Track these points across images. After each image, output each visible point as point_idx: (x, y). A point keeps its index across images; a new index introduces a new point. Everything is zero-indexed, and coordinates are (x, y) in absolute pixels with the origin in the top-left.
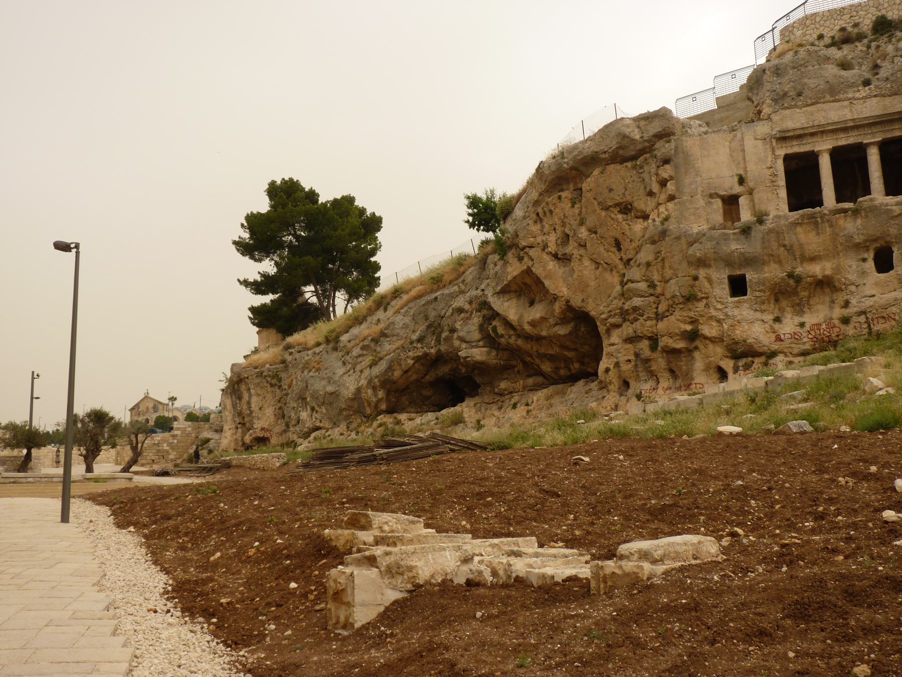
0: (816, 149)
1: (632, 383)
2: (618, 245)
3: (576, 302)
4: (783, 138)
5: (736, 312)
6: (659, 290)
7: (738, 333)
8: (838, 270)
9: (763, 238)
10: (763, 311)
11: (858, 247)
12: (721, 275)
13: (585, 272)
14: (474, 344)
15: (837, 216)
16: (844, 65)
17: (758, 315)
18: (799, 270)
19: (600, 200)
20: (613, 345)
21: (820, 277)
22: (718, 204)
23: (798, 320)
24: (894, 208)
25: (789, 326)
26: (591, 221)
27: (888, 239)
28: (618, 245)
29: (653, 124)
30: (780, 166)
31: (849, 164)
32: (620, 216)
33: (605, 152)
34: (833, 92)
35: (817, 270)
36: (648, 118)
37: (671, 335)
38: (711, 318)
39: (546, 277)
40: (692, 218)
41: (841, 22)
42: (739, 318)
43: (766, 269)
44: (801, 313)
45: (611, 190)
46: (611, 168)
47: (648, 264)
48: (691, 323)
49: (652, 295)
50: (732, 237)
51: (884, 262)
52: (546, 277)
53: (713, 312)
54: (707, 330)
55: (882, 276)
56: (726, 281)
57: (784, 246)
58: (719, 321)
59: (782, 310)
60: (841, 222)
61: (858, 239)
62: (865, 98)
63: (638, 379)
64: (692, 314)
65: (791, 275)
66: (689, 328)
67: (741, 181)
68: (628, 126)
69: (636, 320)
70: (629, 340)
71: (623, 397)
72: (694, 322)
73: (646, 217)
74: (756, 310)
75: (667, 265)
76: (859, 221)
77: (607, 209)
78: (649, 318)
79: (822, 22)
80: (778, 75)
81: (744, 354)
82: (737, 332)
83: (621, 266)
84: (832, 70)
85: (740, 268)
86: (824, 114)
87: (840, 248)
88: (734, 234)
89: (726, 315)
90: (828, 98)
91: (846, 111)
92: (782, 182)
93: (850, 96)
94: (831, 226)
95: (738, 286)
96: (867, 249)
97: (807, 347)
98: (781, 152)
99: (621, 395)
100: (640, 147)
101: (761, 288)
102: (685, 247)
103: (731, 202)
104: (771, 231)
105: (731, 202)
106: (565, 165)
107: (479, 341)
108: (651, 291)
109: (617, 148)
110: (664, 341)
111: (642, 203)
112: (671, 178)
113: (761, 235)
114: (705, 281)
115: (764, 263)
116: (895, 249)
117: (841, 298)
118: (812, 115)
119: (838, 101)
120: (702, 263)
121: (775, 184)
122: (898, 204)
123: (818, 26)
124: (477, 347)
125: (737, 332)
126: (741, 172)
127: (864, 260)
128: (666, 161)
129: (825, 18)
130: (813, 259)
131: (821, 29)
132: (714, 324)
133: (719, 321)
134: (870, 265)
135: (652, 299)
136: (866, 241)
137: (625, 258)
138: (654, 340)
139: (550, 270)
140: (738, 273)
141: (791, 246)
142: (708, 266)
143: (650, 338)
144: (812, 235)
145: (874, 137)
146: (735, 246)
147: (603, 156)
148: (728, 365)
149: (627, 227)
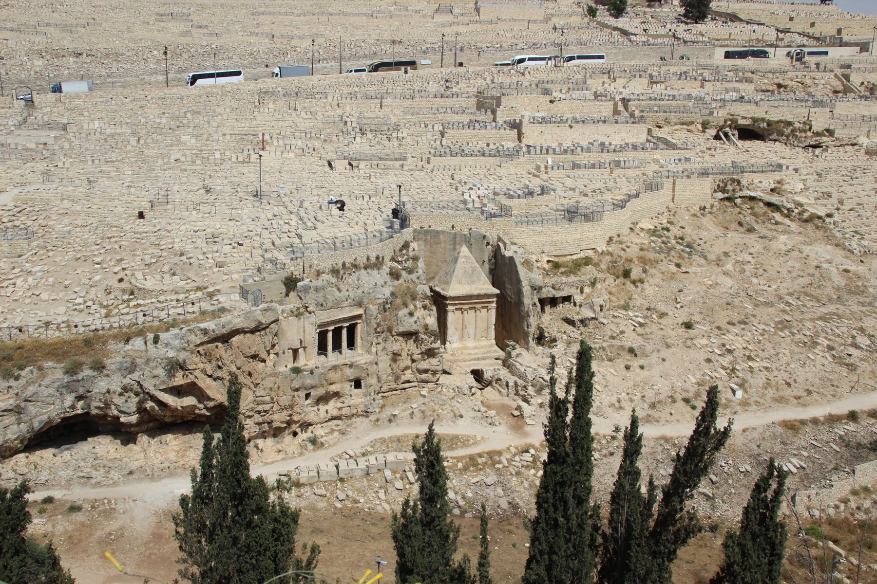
2: (250, 374)
7: (306, 419)
8: (342, 388)
11: (351, 381)
12: (302, 394)
25: (322, 413)
26: (239, 364)
28: (250, 374)
34: (337, 305)
35: (334, 388)
46: (248, 335)
47: (271, 389)
54: (296, 418)
55: (358, 391)
61: (352, 378)
70: (258, 424)
73: (264, 361)
75: (281, 389)
83: (252, 386)
95: (308, 396)
103: (295, 352)
105: (295, 352)
111: (263, 355)
117: (341, 399)
120: (297, 390)
128: (276, 335)
130: (331, 384)
137: (255, 382)
143: (269, 423)
146: (309, 381)
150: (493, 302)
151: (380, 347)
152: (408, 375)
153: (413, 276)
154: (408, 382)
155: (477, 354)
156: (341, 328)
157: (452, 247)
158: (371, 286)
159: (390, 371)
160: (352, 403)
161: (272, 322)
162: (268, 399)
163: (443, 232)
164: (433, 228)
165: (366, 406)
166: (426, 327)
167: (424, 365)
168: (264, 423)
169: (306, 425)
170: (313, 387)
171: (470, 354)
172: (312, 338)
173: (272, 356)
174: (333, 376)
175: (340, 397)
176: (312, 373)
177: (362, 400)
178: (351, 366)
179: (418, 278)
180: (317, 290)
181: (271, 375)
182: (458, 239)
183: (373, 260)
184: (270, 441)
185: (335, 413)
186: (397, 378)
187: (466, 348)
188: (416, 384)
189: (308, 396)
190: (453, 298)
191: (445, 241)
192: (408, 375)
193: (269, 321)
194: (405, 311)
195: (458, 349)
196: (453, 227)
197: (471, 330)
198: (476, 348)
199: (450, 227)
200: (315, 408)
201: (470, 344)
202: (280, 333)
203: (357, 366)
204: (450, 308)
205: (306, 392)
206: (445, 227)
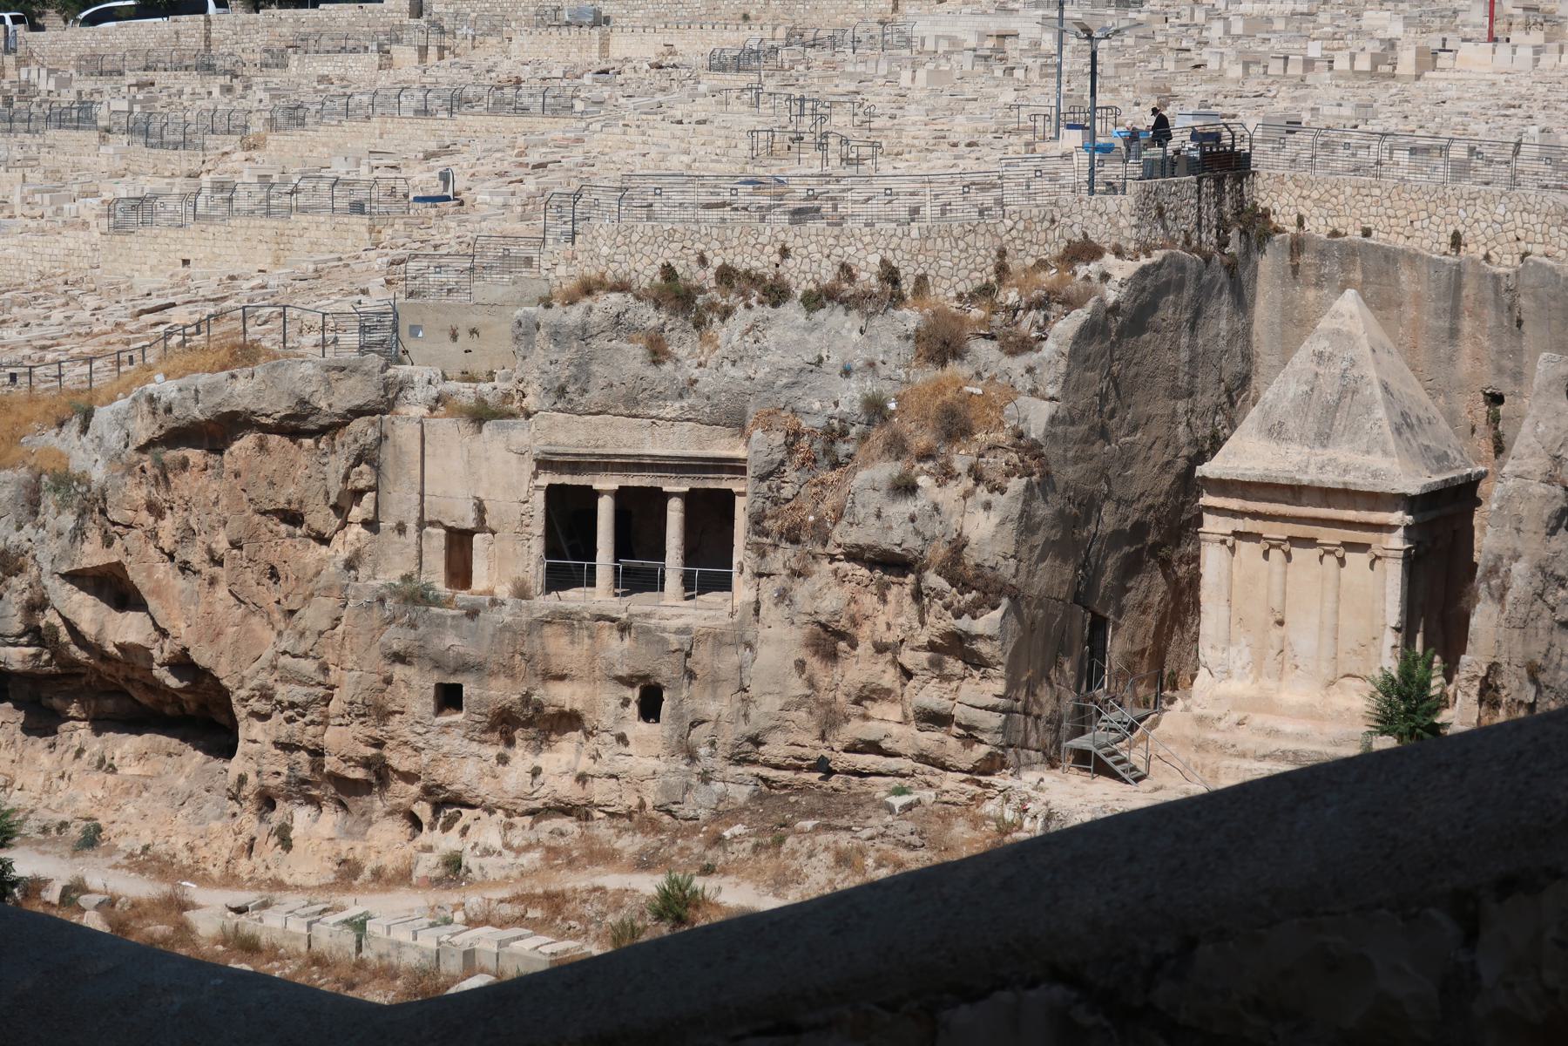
0: (596, 486)
1: (280, 803)
3: (202, 656)
4: (545, 464)
5: (444, 739)
6: (333, 677)
7: (441, 774)
8: (592, 704)
9: (493, 636)
10: (482, 742)
13: (219, 608)
14: (11, 640)
15: (601, 623)
16: (657, 352)
17: (474, 747)
18: (538, 694)
19: (253, 496)
20: (255, 742)
21: (567, 709)
22: (437, 537)
23: (531, 760)
24: (672, 638)
27: (659, 680)
29: (351, 382)
30: (539, 500)
31: (638, 514)
32: (283, 527)
33: (268, 416)
34: (632, 403)
35: (563, 695)
36: (343, 369)
37: (345, 759)
38: (406, 743)
39: (153, 592)
40: (398, 559)
41: (667, 253)
42: (446, 749)
43: (493, 683)
44: (538, 750)
45: (272, 484)
46: (274, 440)
48: (374, 746)
49: (319, 684)
50: (449, 621)
51: (650, 708)
52: (153, 592)
53: (412, 738)
54: (398, 760)
55: (644, 727)
56: (432, 692)
57: (522, 654)
58: (416, 749)
59: (510, 743)
60: (606, 633)
61: (623, 671)
62: (675, 420)
63: (288, 798)
64: (377, 733)
65: (526, 699)
66: (370, 751)
67: (481, 509)
68: (306, 379)
69: (290, 720)
71: (264, 826)
72: (379, 744)
73: (324, 540)
74: (472, 740)
76: (627, 641)
77: (264, 513)
78: (312, 722)
79: (640, 245)
80: (557, 343)
81: (448, 803)
82: (442, 771)
83: (277, 616)
84: (633, 356)
85: (455, 672)
86: (613, 432)
87: (598, 673)
88: (454, 617)
89: (427, 742)
90: (622, 409)
91: (646, 433)
92: (538, 527)
93: (653, 413)
94: (591, 637)
95: (449, 697)
96: (632, 685)
97: (537, 805)
98: (546, 479)
99: (261, 819)
100: (325, 421)
101: (484, 710)
102: (377, 623)
103: (459, 542)
104: (506, 628)
106: (197, 413)
107: (20, 636)
108: (321, 678)
109: (287, 417)
110: (331, 763)
112: (371, 489)
113: (489, 630)
114: (402, 685)
115: (492, 674)
116: (665, 695)
118: (596, 429)
119: (635, 416)
120: (399, 658)
121: (529, 530)
122: (680, 631)
123: (633, 250)
124: (15, 645)
125: (442, 771)
126: (482, 495)
127: (626, 703)
129: (645, 239)
130: (561, 678)
131: (638, 256)
132: (409, 751)
133: (416, 749)
134: (633, 708)
135: (321, 691)
136: (632, 676)
138: (317, 753)
139: (158, 580)
140: (453, 680)
141: (532, 657)
142: (410, 664)
143: (312, 753)
144: (564, 640)
145: (678, 484)
146: (451, 642)
147: (264, 420)
148: (424, 810)
149: (291, 551)
150: (1390, 528)
151: (769, 588)
152: (886, 721)
153: (1018, 364)
154: (873, 747)
155: (1300, 737)
156: (658, 499)
157: (1444, 323)
158: (791, 361)
159: (797, 687)
160: (621, 765)
161: (357, 412)
162: (308, 666)
163: (1413, 258)
164: (1377, 238)
165: (666, 789)
166: (958, 546)
167: (931, 695)
168: (298, 748)
169: (448, 803)
170: (464, 667)
171: (1274, 733)
172: (519, 502)
173: (355, 531)
174: (561, 648)
175: (589, 734)
176: (473, 613)
177: (660, 766)
178: (624, 628)
179: (1030, 370)
180: (557, 335)
181: (328, 590)
182: (1469, 291)
183: (868, 278)
184: (330, 819)
185: (567, 789)
186: (830, 722)
187: (1266, 705)
188: (905, 765)
189: (449, 697)
190: (1224, 487)
191: (1418, 297)
192: (886, 721)
193: (341, 406)
194: (887, 470)
195: (1236, 703)
196: (1456, 241)
197: (1305, 636)
198: (1308, 713)
199: (1446, 239)
200: (491, 752)
201: (1296, 692)
202: (387, 454)
203: (647, 631)
204: (1211, 524)
205: (436, 677)
206: (1431, 241)
